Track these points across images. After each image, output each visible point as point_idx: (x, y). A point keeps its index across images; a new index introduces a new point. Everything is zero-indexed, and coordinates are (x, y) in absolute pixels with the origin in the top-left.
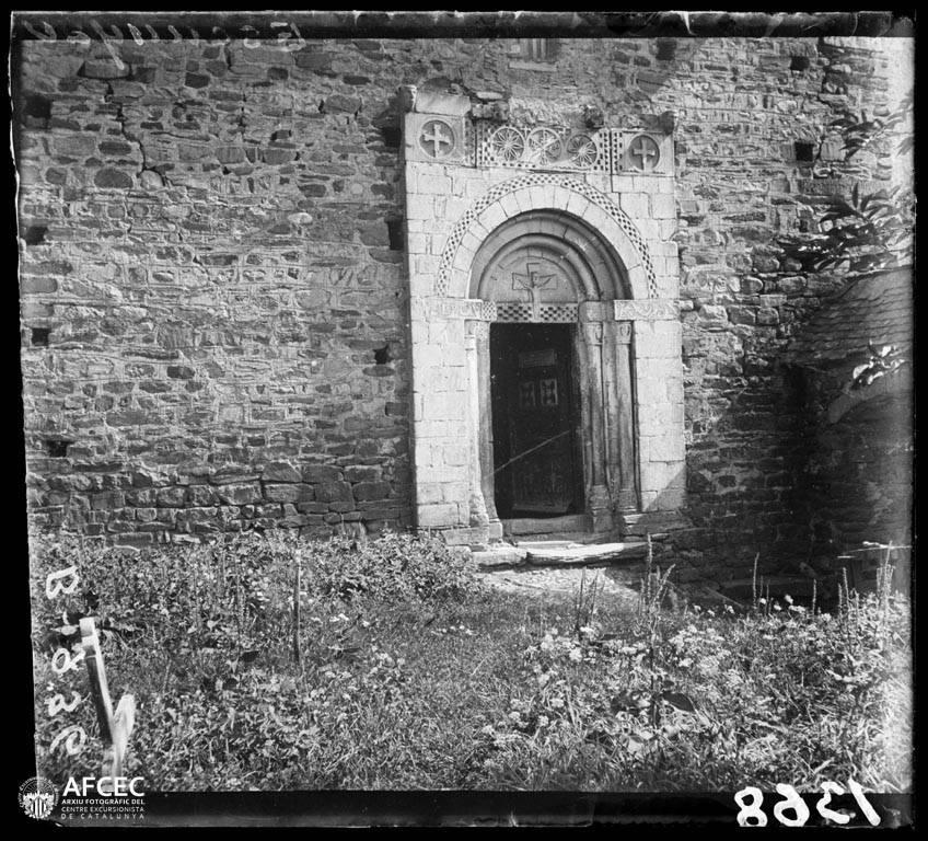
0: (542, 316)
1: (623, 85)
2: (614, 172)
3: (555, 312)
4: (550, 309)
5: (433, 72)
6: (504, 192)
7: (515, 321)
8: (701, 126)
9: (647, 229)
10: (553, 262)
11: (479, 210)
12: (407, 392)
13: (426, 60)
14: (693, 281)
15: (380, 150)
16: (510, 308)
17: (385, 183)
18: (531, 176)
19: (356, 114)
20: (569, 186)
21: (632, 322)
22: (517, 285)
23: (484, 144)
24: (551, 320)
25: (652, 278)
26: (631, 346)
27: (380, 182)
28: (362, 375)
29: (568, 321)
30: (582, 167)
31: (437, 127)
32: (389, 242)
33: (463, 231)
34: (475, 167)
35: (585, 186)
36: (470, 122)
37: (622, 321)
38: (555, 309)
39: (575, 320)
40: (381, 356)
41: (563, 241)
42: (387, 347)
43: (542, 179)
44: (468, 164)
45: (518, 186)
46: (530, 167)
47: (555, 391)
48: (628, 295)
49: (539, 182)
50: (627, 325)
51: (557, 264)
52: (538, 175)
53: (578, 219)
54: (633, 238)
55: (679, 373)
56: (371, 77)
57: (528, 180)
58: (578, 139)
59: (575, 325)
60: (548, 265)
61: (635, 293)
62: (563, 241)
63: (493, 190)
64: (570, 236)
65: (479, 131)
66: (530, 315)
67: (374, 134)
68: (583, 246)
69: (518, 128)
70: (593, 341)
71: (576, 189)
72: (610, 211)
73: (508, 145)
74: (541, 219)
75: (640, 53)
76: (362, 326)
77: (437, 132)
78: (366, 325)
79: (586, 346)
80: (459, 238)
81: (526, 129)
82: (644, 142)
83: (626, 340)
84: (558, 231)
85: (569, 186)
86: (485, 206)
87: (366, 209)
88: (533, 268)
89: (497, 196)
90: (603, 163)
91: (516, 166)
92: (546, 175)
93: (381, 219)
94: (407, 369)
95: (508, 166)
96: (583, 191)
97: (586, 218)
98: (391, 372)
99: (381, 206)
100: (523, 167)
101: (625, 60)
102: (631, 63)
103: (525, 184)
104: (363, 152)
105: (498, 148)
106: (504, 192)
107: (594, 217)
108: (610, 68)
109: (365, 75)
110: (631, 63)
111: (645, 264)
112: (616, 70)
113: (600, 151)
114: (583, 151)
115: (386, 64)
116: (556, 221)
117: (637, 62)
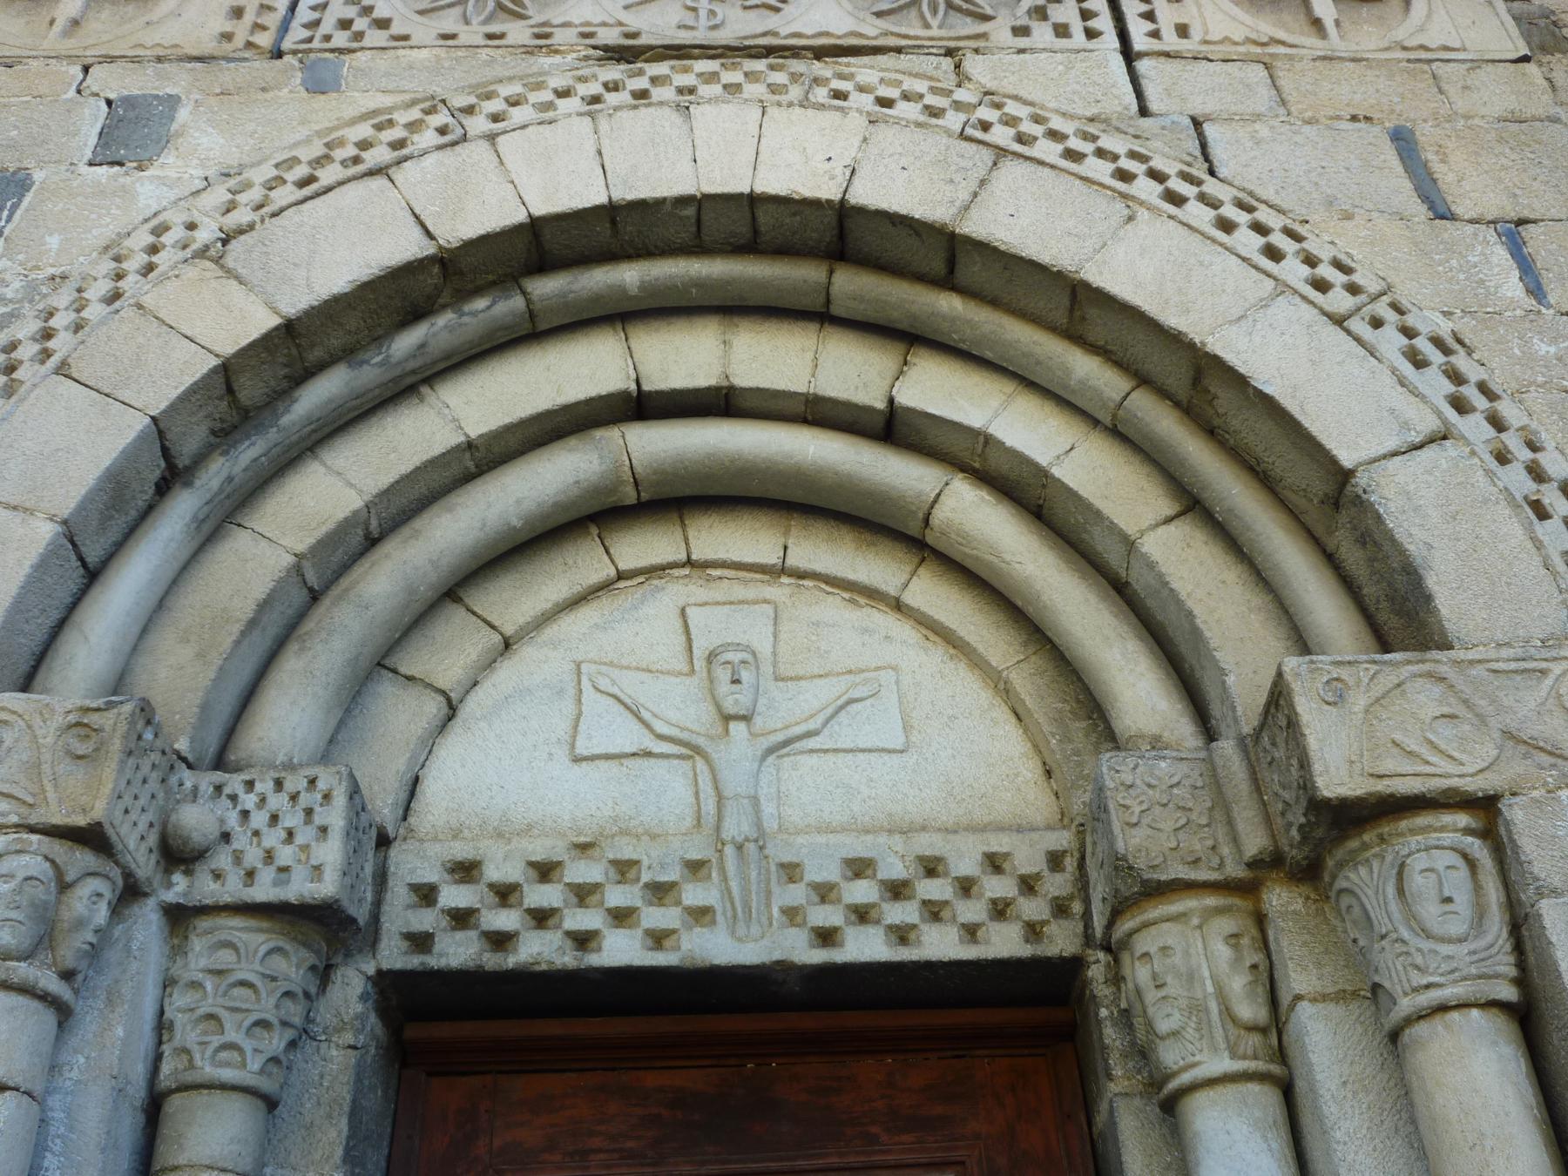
0: (792, 914)
2: (1140, 42)
3: (897, 890)
7: (568, 959)
10: (872, 594)
11: (242, 216)
16: (545, 871)
18: (614, 72)
24: (865, 946)
29: (1005, 943)
30: (935, 32)
35: (962, 95)
38: (894, 869)
39: (1061, 941)
41: (891, 428)
46: (610, 37)
51: (898, 606)
59: (1073, 967)
60: (833, 608)
61: (1451, 599)
62: (891, 428)
66: (701, 915)
68: (1028, 431)
70: (1197, 1053)
84: (851, 370)
88: (711, 627)
95: (472, 34)
100: (560, 37)
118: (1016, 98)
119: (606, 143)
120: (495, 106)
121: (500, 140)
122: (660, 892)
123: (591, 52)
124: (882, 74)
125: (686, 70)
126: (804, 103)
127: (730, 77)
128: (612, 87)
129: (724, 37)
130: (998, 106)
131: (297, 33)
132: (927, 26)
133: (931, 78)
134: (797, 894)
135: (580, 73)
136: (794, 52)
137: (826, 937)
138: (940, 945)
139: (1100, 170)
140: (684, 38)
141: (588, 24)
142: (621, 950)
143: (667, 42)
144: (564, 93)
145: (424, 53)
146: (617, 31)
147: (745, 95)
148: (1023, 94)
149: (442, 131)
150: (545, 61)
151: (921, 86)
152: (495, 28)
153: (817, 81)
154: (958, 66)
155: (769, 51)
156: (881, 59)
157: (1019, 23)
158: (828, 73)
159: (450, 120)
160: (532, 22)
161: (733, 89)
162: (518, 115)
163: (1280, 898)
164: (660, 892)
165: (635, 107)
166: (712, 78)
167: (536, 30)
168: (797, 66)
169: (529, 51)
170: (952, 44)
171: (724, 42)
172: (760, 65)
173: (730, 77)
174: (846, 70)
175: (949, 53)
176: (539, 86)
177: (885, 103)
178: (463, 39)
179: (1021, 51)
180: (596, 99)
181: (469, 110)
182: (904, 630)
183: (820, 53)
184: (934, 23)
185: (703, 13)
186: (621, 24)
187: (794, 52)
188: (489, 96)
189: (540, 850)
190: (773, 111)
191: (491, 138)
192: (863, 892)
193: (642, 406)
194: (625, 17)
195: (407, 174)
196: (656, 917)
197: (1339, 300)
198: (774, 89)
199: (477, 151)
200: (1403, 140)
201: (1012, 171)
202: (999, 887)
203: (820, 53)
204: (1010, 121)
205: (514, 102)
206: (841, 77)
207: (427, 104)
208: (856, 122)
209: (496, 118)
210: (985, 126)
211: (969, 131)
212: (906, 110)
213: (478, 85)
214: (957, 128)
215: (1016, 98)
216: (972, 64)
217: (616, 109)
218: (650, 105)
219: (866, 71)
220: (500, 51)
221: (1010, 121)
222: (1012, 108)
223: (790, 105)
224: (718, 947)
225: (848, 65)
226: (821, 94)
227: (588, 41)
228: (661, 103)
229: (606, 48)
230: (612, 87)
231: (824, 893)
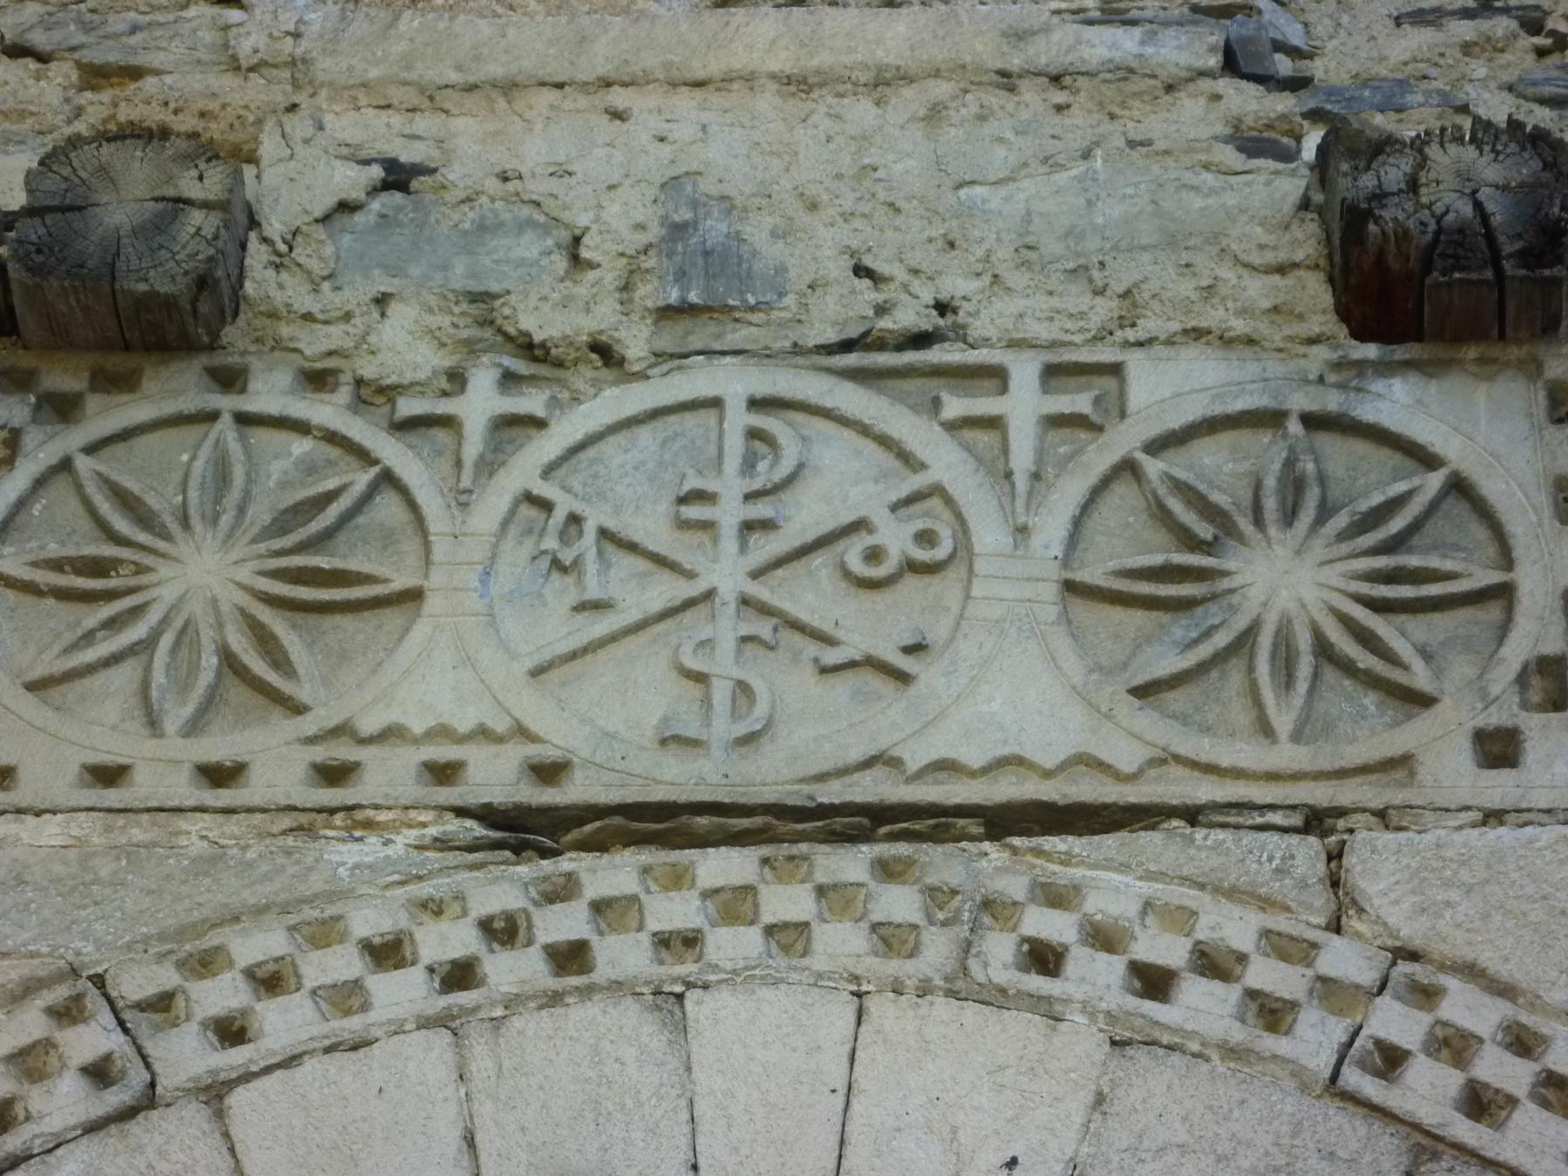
18: (503, 887)
20: (1096, 977)
30: (1285, 755)
35: (1346, 960)
43: (675, 911)
45: (283, 1022)
46: (495, 778)
49: (623, 955)
52: (614, 873)
58: (1218, 466)
69: (372, 395)
71: (1202, 1006)
73: (205, 576)
85: (1096, 977)
95: (163, 772)
100: (387, 776)
114: (1288, 579)
118: (1471, 972)
119: (485, 1111)
120: (221, 994)
121: (238, 1099)
123: (454, 826)
124: (1146, 888)
125: (678, 879)
126: (959, 986)
127: (787, 901)
128: (503, 931)
129: (771, 776)
130: (1426, 995)
132: (1265, 729)
133: (1266, 903)
135: (425, 890)
136: (935, 823)
140: (675, 778)
141: (442, 733)
143: (633, 795)
144: (387, 953)
145: (51, 831)
146: (516, 754)
147: (818, 962)
148: (1488, 958)
149: (100, 1073)
150: (344, 854)
151: (1236, 928)
152: (217, 747)
153: (992, 907)
154: (1335, 855)
156: (1149, 843)
157: (1494, 718)
158: (1015, 887)
159: (114, 1042)
160: (309, 724)
161: (789, 937)
162: (283, 1022)
165: (555, 999)
166: (734, 904)
167: (320, 754)
168: (944, 863)
169: (307, 823)
170: (1319, 795)
171: (769, 795)
172: (850, 864)
173: (787, 901)
174: (1064, 875)
175: (1315, 821)
176: (324, 934)
177: (1153, 982)
178: (144, 787)
179: (1492, 817)
180: (460, 975)
181: (162, 1003)
183: (1003, 822)
184: (1283, 723)
185: (721, 693)
186: (522, 732)
187: (935, 823)
188: (206, 964)
190: (882, 1008)
191: (214, 1093)
194: (534, 709)
198: (892, 939)
199: (180, 1132)
203: (1003, 822)
204: (1453, 1045)
205: (270, 981)
206: (1055, 897)
207: (60, 993)
208: (1081, 1042)
209: (231, 1032)
210: (1390, 1060)
211: (1353, 1078)
212: (1202, 1006)
213: (182, 933)
214: (1321, 1063)
215: (1471, 972)
216: (1378, 864)
217: (513, 1003)
218: (587, 992)
219: (1112, 879)
220: (234, 825)
221: (1453, 1045)
222: (1466, 1008)
223: (924, 990)
225: (1067, 860)
226: (998, 955)
227: (446, 795)
228: (617, 987)
229: (486, 814)
230: (503, 931)
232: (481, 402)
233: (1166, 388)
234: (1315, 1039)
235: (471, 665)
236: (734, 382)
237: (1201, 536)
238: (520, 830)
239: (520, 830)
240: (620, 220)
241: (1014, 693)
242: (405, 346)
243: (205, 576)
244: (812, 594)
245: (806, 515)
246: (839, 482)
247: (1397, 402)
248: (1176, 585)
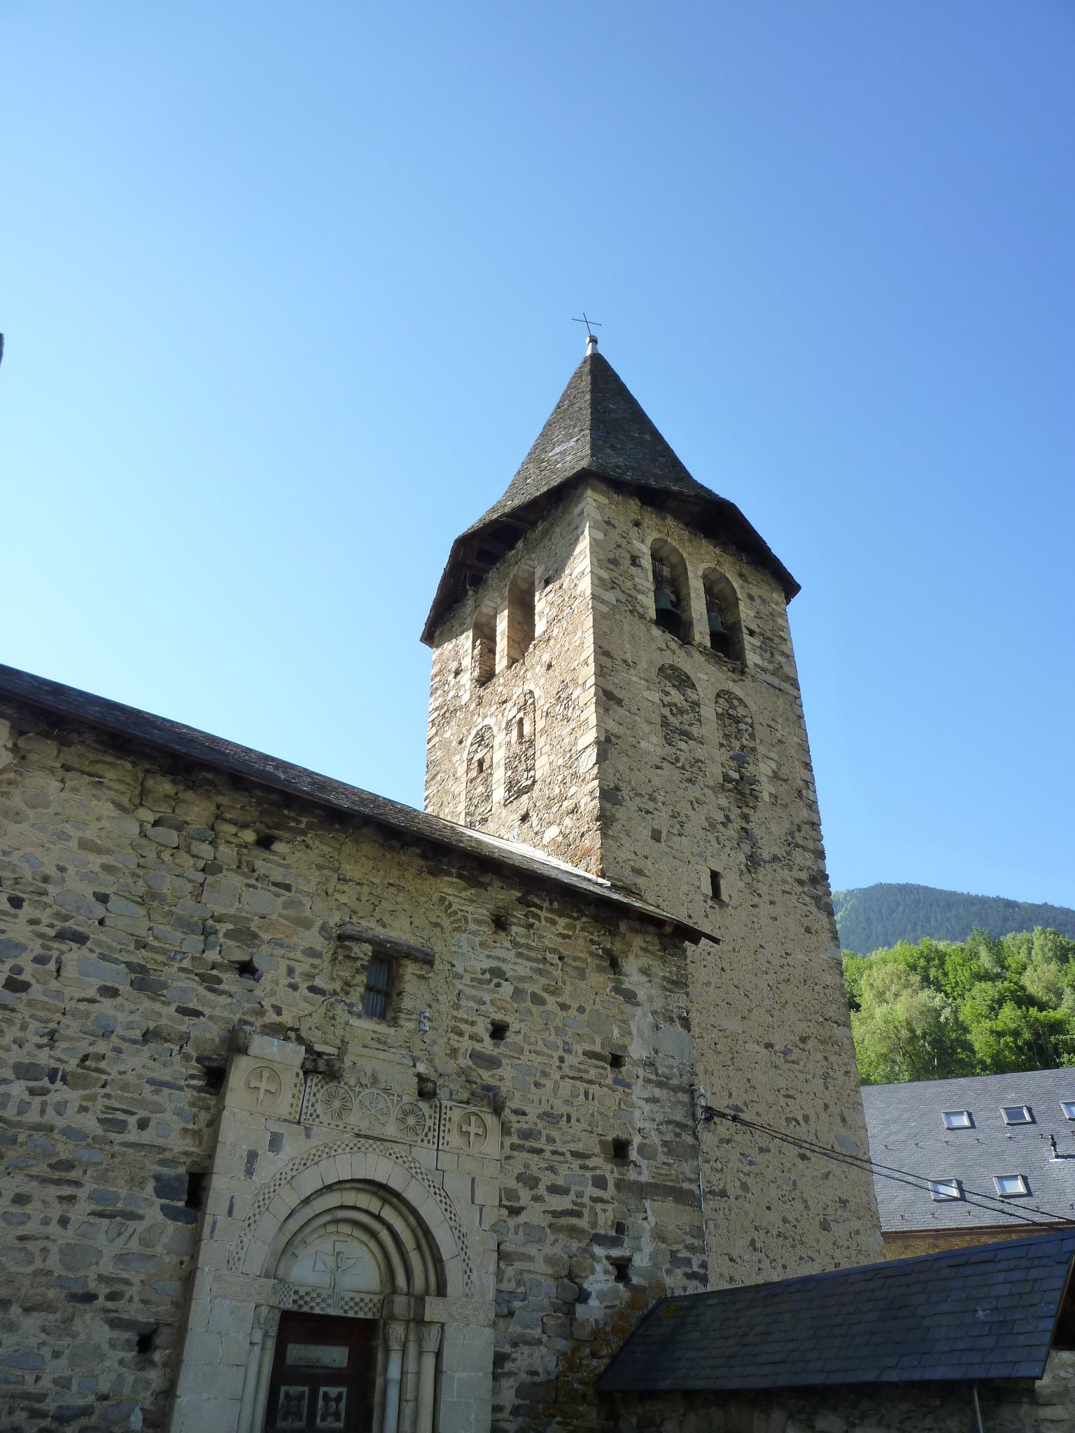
1: (456, 1058)
3: (356, 1304)
4: (352, 1299)
5: (271, 1017)
6: (325, 1155)
8: (527, 1110)
9: (469, 1217)
11: (295, 1173)
12: (168, 1393)
13: (267, 1004)
14: (509, 1280)
15: (200, 1089)
17: (196, 1127)
19: (181, 1047)
21: (443, 1325)
22: (320, 1266)
23: (313, 1100)
24: (351, 1314)
25: (468, 1272)
26: (438, 1355)
27: (191, 1126)
28: (116, 1365)
29: (370, 1316)
31: (266, 1074)
32: (185, 1197)
33: (272, 1195)
34: (299, 1123)
36: (301, 1075)
37: (431, 1323)
38: (357, 1300)
40: (145, 1344)
41: (378, 1218)
42: (155, 1331)
44: (291, 1118)
45: (340, 1150)
47: (343, 1405)
48: (441, 1291)
50: (438, 1327)
53: (397, 1195)
54: (452, 1223)
55: (488, 1396)
56: (207, 1011)
57: (351, 1145)
60: (356, 1243)
62: (378, 1218)
63: (314, 1151)
64: (389, 1214)
65: (309, 1083)
66: (329, 1305)
67: (195, 1072)
68: (399, 1226)
70: (395, 1346)
72: (432, 1190)
73: (337, 1104)
74: (359, 1190)
75: (474, 1029)
76: (131, 1300)
77: (265, 1079)
78: (136, 1299)
79: (387, 1351)
80: (267, 1202)
81: (357, 1089)
82: (473, 1119)
83: (431, 1344)
86: (301, 1168)
87: (168, 1155)
88: (339, 1247)
89: (316, 1159)
90: (430, 1136)
91: (341, 1127)
92: (371, 1142)
93: (182, 1170)
94: (174, 1366)
96: (407, 1165)
97: (408, 1196)
98: (152, 1363)
99: (186, 1153)
100: (349, 1129)
101: (461, 1034)
102: (466, 1037)
103: (348, 1149)
104: (180, 1089)
105: (328, 1102)
106: (325, 1155)
107: (414, 1194)
108: (445, 1040)
109: (200, 1008)
110: (466, 1037)
111: (463, 1255)
112: (452, 1042)
113: (429, 1123)
115: (223, 1000)
116: (374, 1194)
117: (471, 1038)
122: (323, 1300)
129: (375, 1134)
131: (303, 1117)
134: (343, 1303)
137: (346, 1311)
138: (361, 1315)
139: (426, 1183)
142: (317, 1311)
155: (380, 1139)
163: (412, 1324)
164: (323, 1300)
182: (366, 1249)
189: (308, 1290)
192: (352, 1304)
193: (342, 1207)
195: (321, 1164)
196: (324, 1305)
197: (452, 1223)
200: (473, 1180)
201: (414, 1181)
202: (371, 1305)
219: (396, 1147)
224: (331, 1312)
231: (346, 1303)
232: (357, 1089)
233: (406, 1099)
234: (407, 1165)
235: (354, 1119)
236: (376, 1091)
237: (406, 1114)
238: (358, 1135)
239: (358, 1135)
240: (369, 1073)
241: (392, 1130)
242: (352, 1082)
243: (337, 1104)
244: (379, 1116)
245: (379, 1107)
246: (381, 1104)
247: (420, 1104)
248: (403, 1120)
